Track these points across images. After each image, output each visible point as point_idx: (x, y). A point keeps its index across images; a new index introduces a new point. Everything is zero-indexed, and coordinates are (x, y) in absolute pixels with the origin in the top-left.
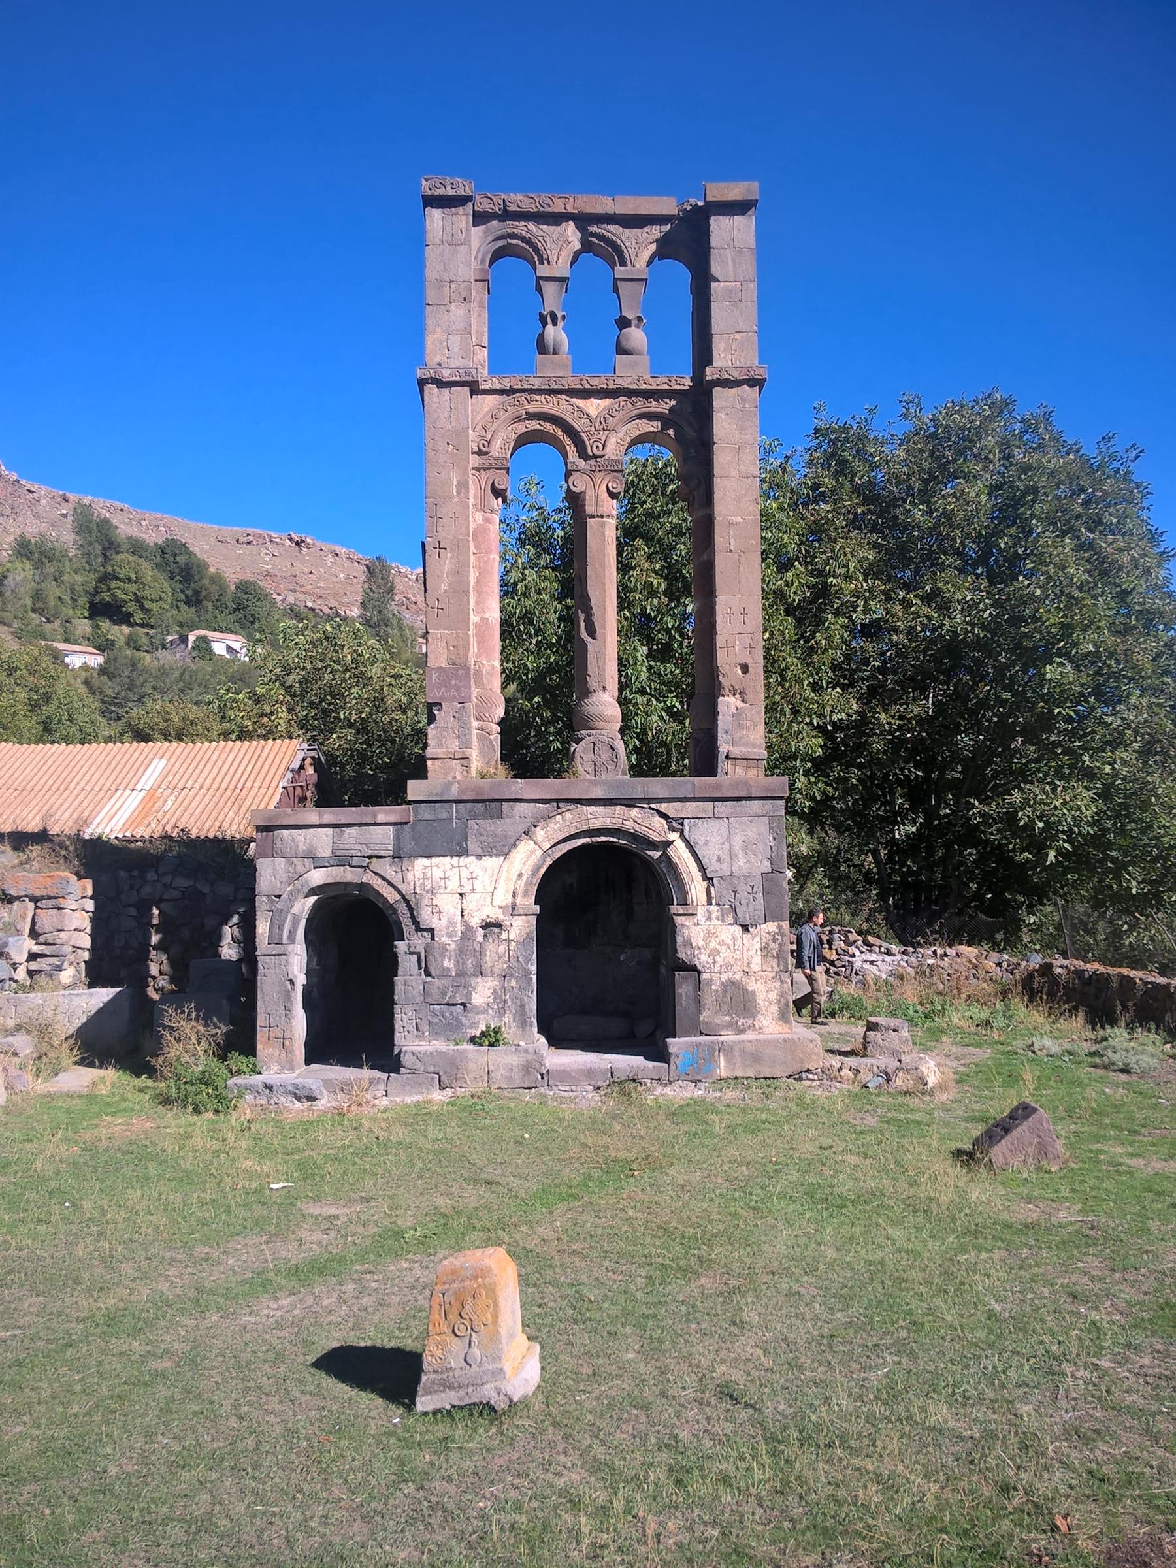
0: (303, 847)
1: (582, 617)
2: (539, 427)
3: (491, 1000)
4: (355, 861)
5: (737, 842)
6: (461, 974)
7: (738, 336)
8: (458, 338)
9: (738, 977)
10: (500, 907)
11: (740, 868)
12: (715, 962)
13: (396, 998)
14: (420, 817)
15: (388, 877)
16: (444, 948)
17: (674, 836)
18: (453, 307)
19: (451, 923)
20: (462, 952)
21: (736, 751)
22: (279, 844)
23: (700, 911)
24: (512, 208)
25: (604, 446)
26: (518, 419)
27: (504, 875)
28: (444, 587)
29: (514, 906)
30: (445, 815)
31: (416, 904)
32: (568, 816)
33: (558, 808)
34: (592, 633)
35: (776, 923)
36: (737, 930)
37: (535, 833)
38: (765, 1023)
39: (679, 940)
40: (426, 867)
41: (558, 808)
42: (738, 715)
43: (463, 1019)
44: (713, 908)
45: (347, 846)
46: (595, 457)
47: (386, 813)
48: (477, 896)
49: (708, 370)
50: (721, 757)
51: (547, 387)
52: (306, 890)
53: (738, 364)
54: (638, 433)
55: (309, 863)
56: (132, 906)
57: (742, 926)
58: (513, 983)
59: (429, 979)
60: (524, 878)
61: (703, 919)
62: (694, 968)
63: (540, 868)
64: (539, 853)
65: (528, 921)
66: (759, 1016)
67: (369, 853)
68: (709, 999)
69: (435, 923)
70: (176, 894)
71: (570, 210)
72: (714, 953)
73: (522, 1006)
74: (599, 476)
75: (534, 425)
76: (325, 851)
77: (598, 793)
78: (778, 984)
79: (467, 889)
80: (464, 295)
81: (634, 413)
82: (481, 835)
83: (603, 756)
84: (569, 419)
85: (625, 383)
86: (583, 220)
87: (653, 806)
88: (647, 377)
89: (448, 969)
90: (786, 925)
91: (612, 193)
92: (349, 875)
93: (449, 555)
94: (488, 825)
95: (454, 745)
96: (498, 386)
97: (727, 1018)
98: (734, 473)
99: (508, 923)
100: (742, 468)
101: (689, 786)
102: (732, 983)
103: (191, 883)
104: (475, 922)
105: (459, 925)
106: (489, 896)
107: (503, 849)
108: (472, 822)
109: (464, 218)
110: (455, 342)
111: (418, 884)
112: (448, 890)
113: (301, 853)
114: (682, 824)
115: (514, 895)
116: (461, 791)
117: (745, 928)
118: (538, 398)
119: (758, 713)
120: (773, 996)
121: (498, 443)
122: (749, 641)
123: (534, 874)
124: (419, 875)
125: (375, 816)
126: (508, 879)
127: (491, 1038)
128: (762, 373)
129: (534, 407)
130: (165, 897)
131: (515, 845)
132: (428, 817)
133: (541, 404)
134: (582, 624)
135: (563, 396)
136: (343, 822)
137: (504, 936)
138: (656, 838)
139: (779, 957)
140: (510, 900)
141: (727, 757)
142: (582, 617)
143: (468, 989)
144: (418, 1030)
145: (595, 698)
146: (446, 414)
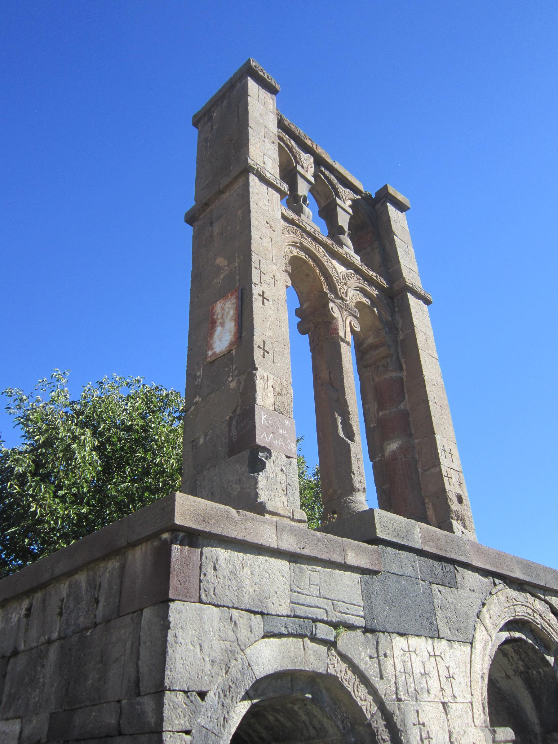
1: (339, 419)
4: (323, 631)
31: (403, 721)
34: (350, 434)
45: (309, 600)
75: (302, 255)
87: (548, 598)
111: (400, 684)
113: (246, 603)
134: (340, 426)
136: (307, 552)
142: (339, 419)
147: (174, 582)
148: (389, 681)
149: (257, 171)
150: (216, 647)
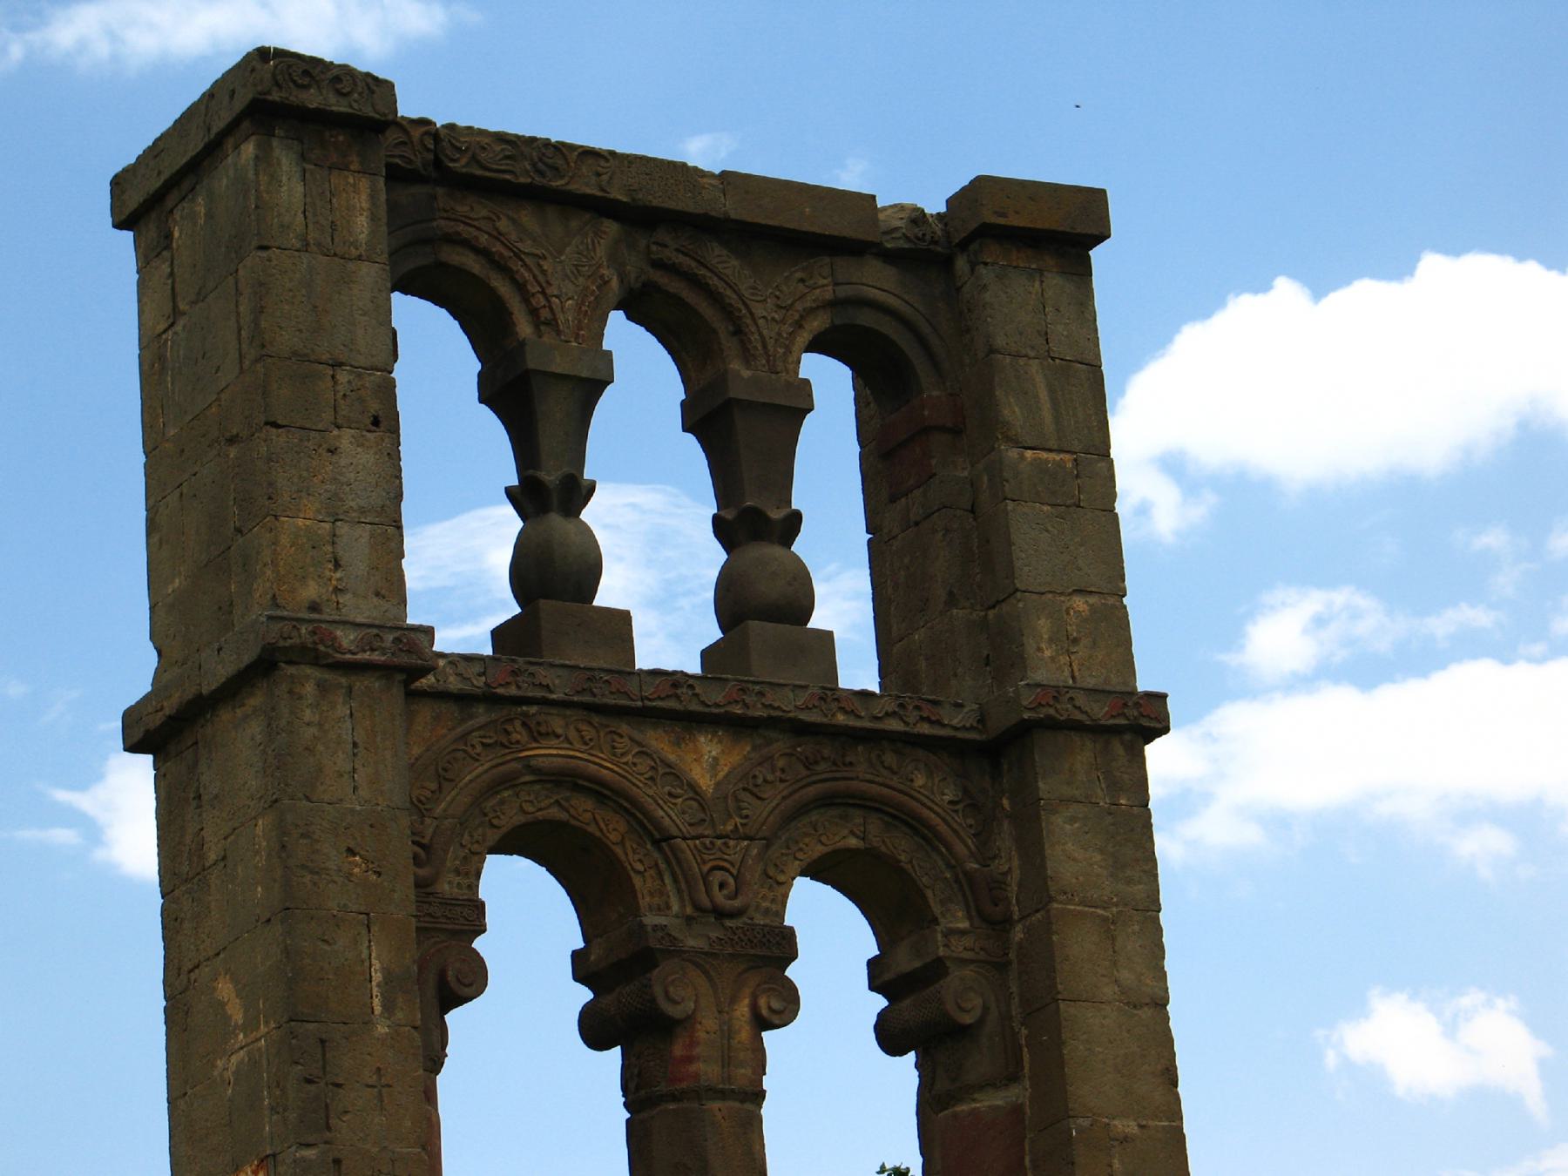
2: (555, 813)
7: (1079, 603)
8: (363, 533)
18: (345, 439)
24: (460, 165)
46: (720, 914)
51: (587, 698)
81: (811, 791)
85: (789, 703)
98: (1109, 991)
100: (1126, 976)
109: (364, 184)
118: (557, 725)
129: (548, 754)
135: (624, 728)
149: (303, 648)
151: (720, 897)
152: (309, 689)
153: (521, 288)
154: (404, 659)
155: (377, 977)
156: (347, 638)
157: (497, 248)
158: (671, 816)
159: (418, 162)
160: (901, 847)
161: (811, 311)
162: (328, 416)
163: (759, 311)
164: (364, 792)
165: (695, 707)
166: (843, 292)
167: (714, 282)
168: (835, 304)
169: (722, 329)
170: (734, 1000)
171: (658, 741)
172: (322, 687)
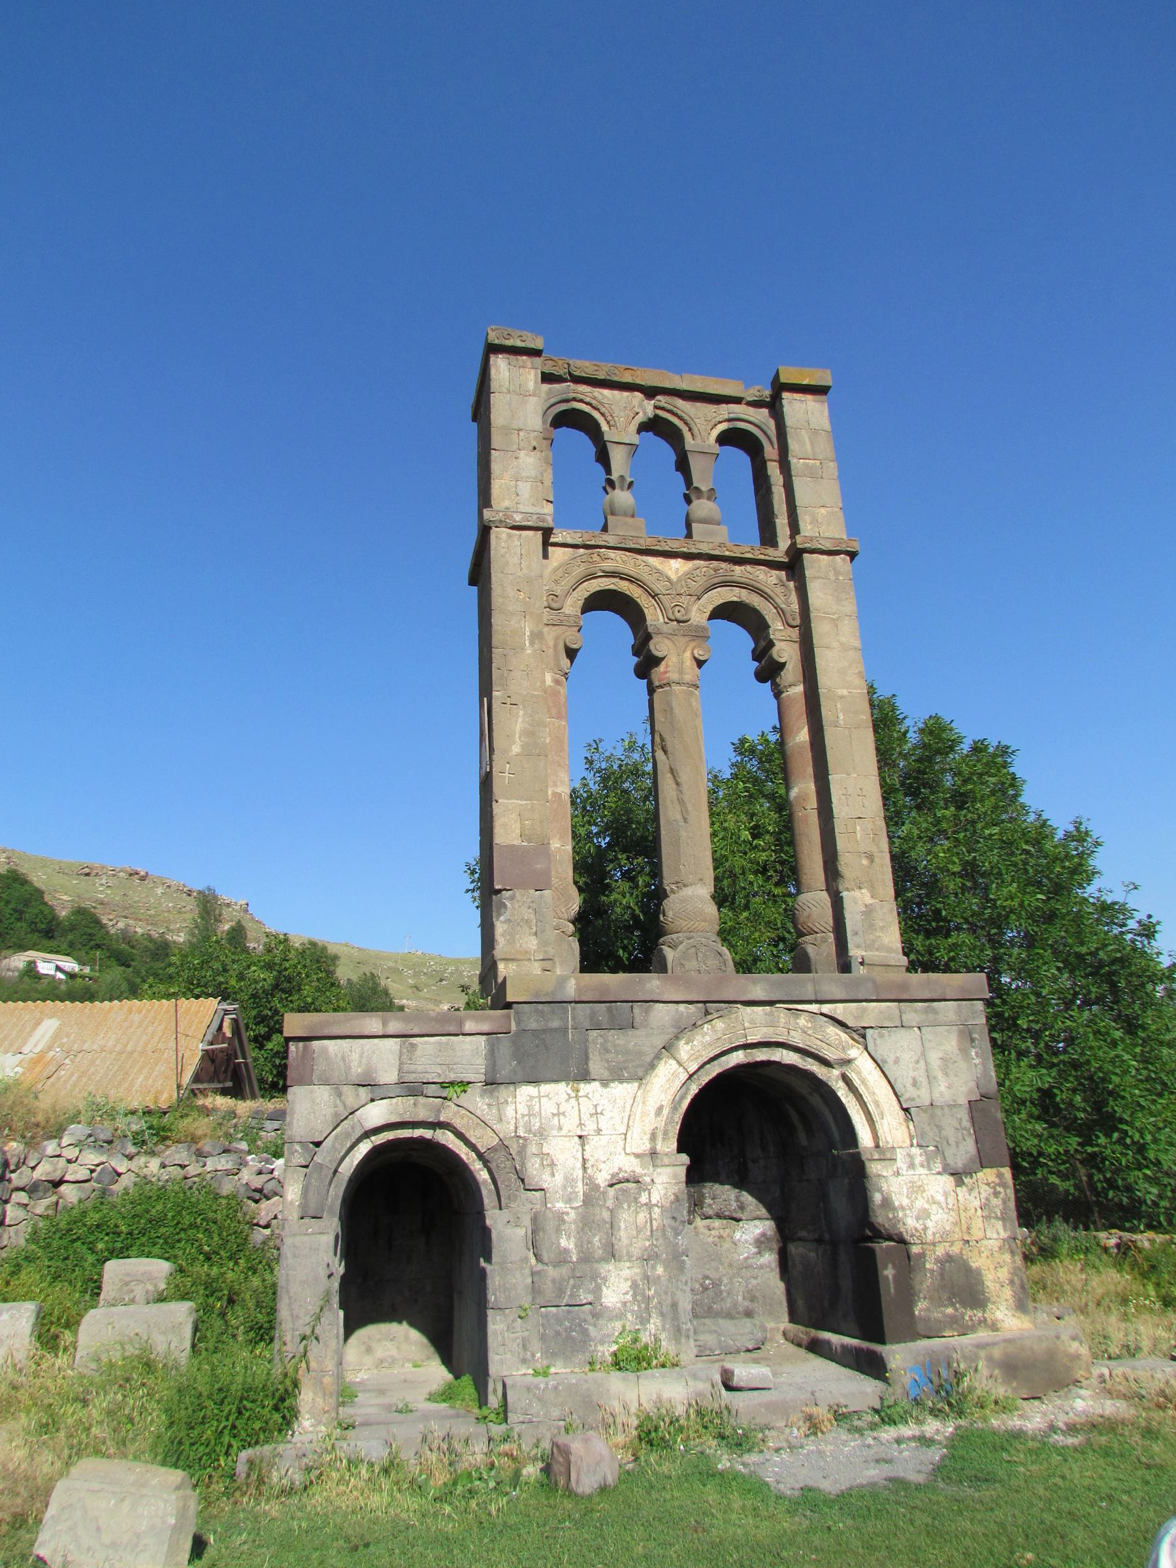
0: (357, 1070)
2: (612, 587)
3: (629, 1297)
5: (934, 1057)
6: (586, 1258)
7: (823, 511)
8: (528, 485)
9: (955, 1249)
10: (637, 1156)
11: (941, 1094)
12: (925, 1229)
13: (491, 1298)
14: (523, 1026)
15: (478, 1113)
16: (560, 1217)
17: (855, 1052)
18: (522, 454)
19: (569, 1180)
20: (586, 1223)
21: (871, 955)
22: (320, 1067)
23: (900, 1154)
25: (687, 611)
26: (592, 576)
27: (638, 1110)
28: (516, 749)
29: (653, 1154)
30: (555, 1024)
32: (719, 1024)
33: (707, 1013)
35: (994, 1170)
36: (948, 1181)
37: (678, 1049)
38: (999, 1315)
39: (877, 1198)
40: (532, 1098)
41: (707, 1013)
42: (869, 911)
43: (591, 1328)
44: (915, 1151)
45: (420, 1068)
46: (679, 622)
47: (477, 1020)
48: (603, 1140)
49: (798, 539)
50: (855, 965)
51: (623, 545)
52: (358, 1133)
53: (826, 535)
54: (721, 601)
55: (364, 1093)
56: (23, 1189)
57: (952, 1174)
58: (660, 1270)
59: (540, 1267)
60: (665, 1112)
61: (904, 1167)
62: (902, 1241)
63: (683, 1097)
64: (684, 1076)
65: (675, 1176)
66: (990, 1306)
67: (452, 1076)
68: (925, 1283)
69: (546, 1180)
70: (83, 1174)
71: (638, 381)
72: (924, 1215)
73: (674, 1305)
74: (682, 641)
76: (388, 1076)
77: (758, 993)
78: (1007, 1257)
79: (590, 1127)
80: (534, 443)
81: (716, 580)
82: (607, 1051)
83: (709, 963)
84: (646, 578)
85: (705, 548)
86: (650, 392)
88: (728, 544)
89: (566, 1251)
90: (1007, 1172)
91: (679, 371)
92: (421, 1109)
93: (521, 713)
94: (617, 1038)
95: (532, 943)
96: (569, 541)
97: (950, 1310)
99: (647, 1179)
100: (843, 639)
101: (870, 984)
102: (949, 1258)
103: (103, 1159)
104: (602, 1179)
105: (580, 1184)
106: (620, 1139)
107: (637, 1071)
108: (594, 1034)
109: (533, 372)
110: (525, 489)
111: (521, 1123)
112: (563, 1133)
113: (354, 1078)
114: (864, 1037)
115: (653, 1137)
116: (579, 989)
117: (958, 1176)
119: (891, 911)
120: (1004, 1274)
121: (569, 601)
122: (870, 826)
123: (674, 1108)
124: (522, 1109)
125: (461, 1023)
126: (644, 1114)
127: (634, 1360)
128: (855, 546)
129: (608, 566)
130: (67, 1178)
131: (652, 1066)
132: (533, 1025)
133: (618, 561)
136: (416, 1031)
137: (644, 1198)
138: (830, 1054)
139: (1003, 1219)
140: (646, 1146)
141: (862, 963)
143: (597, 1282)
144: (525, 1347)
145: (688, 892)
146: (516, 560)
147: (291, 1074)
148: (509, 1123)
150: (328, 1111)
151: (678, 616)
152: (504, 536)
153: (603, 415)
154: (541, 524)
155: (528, 633)
156: (518, 519)
157: (594, 402)
158: (658, 587)
159: (561, 373)
160: (755, 601)
161: (720, 422)
162: (515, 447)
163: (697, 421)
164: (525, 571)
165: (667, 548)
166: (732, 416)
167: (680, 413)
168: (729, 420)
169: (685, 429)
170: (684, 651)
171: (651, 560)
172: (509, 536)
